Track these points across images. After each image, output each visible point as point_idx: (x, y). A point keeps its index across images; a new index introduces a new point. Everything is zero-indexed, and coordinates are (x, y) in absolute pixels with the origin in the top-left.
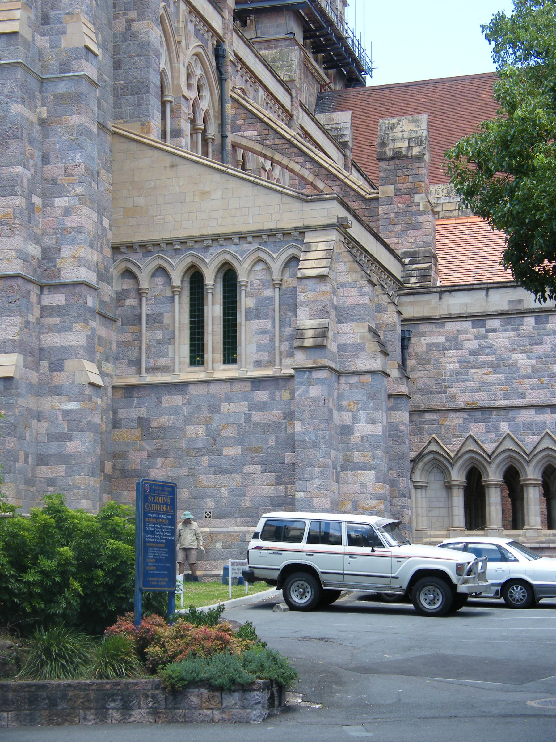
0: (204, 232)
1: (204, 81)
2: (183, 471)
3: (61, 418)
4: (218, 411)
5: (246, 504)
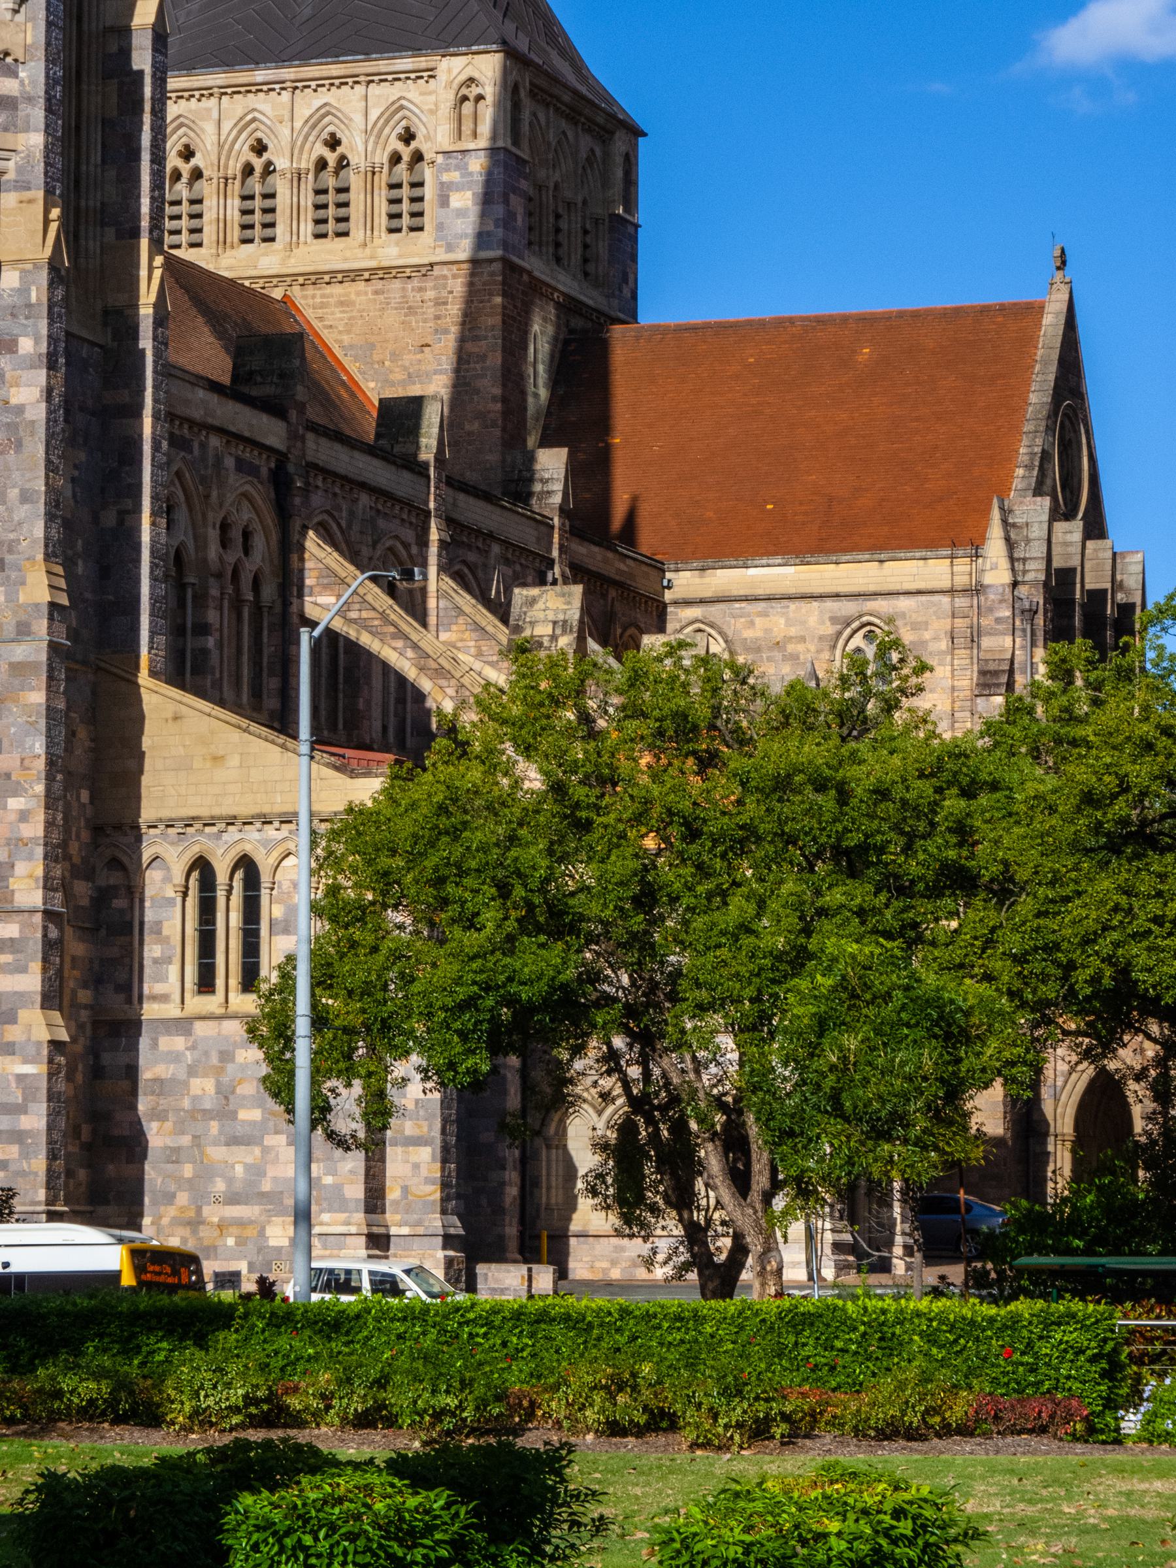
0: (216, 811)
1: (256, 526)
2: (186, 1140)
3: (14, 1085)
4: (233, 1060)
5: (266, 1186)
